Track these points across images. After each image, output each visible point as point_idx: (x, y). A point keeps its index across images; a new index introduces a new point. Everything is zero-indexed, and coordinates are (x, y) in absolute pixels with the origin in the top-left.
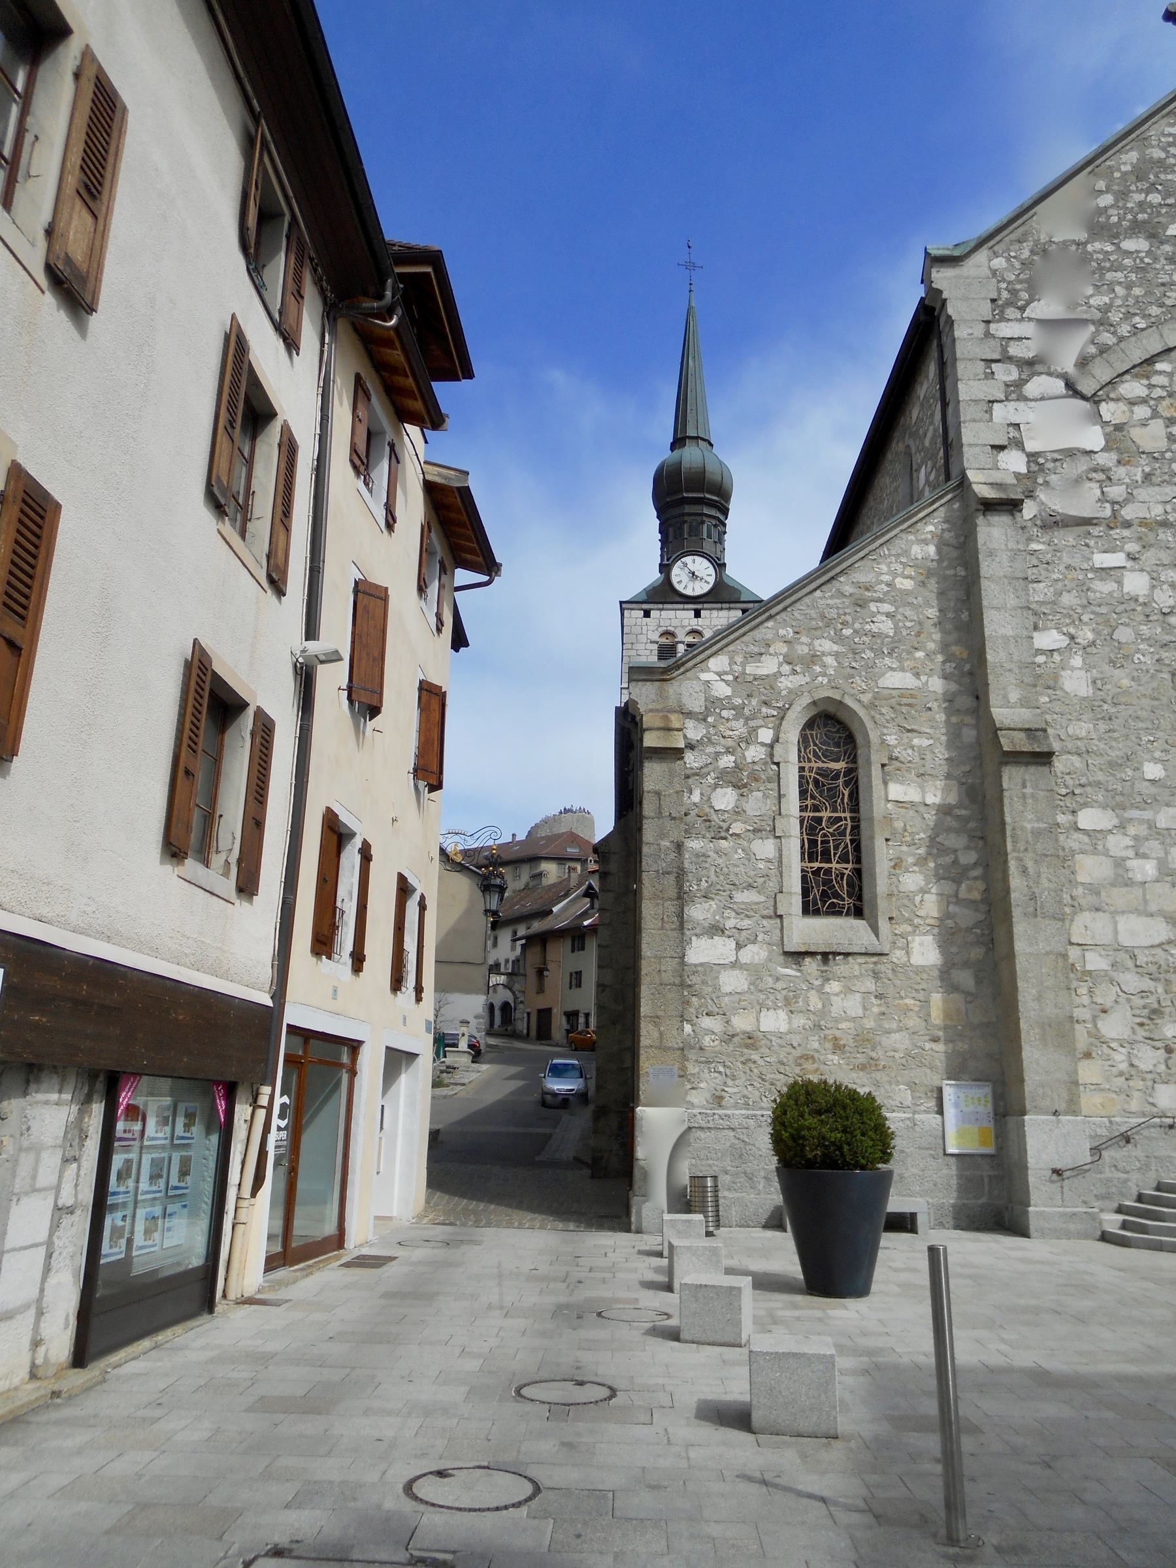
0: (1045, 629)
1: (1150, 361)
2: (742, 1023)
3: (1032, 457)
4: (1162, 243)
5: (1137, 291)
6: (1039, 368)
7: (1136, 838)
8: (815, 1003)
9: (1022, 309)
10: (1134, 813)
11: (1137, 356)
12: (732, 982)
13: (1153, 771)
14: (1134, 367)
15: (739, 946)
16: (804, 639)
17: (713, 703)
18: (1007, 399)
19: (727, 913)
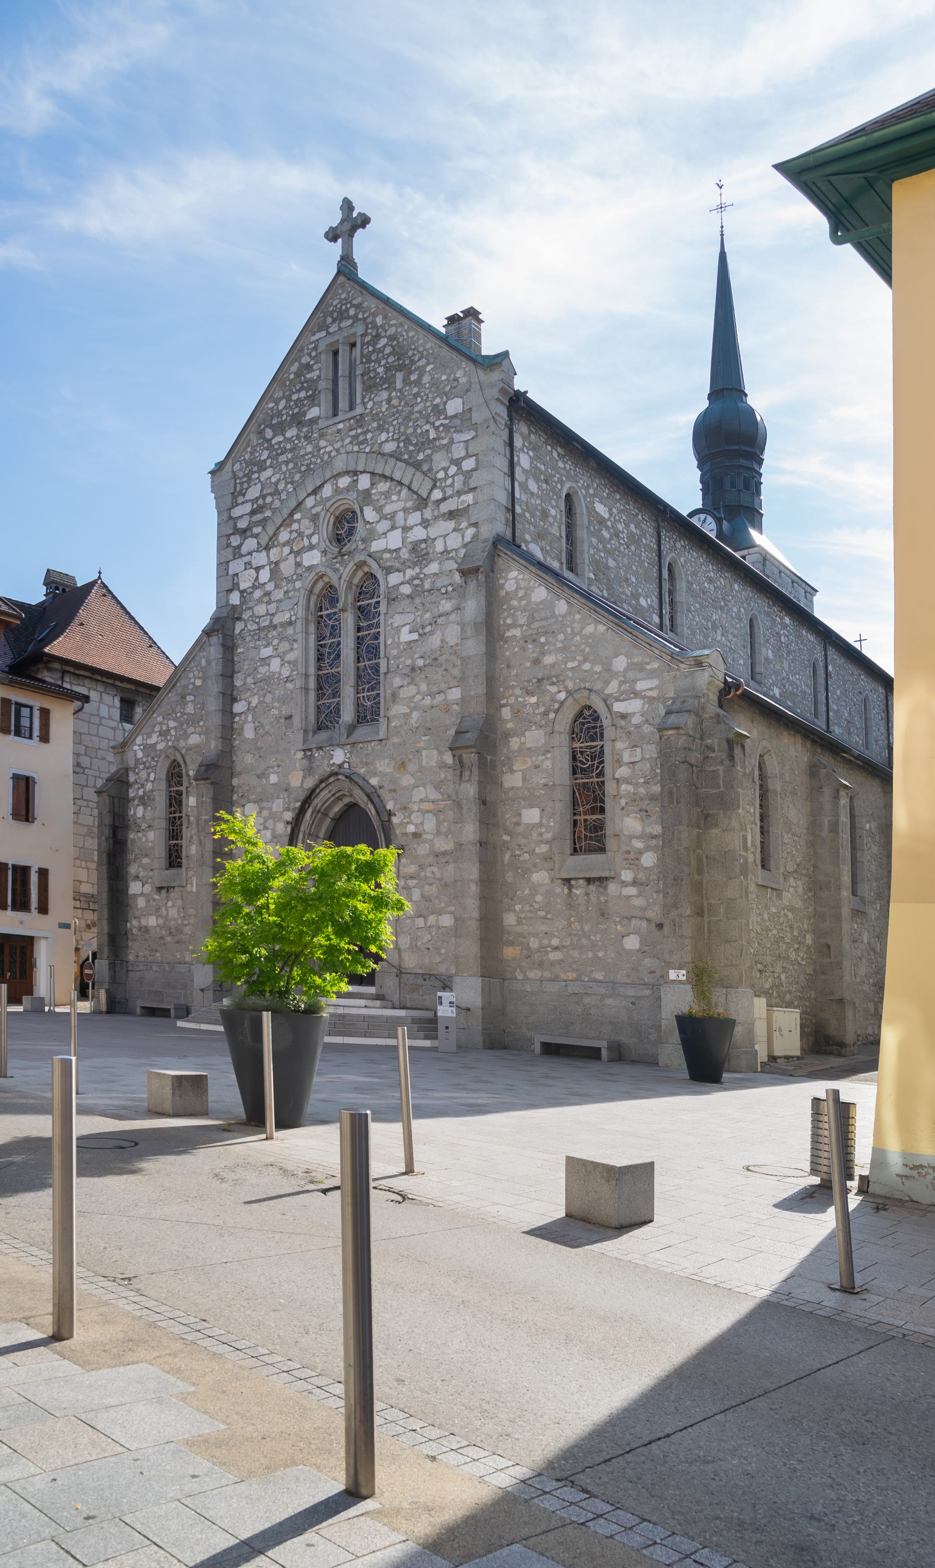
0: (241, 700)
1: (291, 514)
2: (144, 922)
3: (242, 592)
4: (303, 426)
5: (291, 465)
6: (249, 533)
7: (264, 818)
8: (164, 913)
9: (244, 495)
10: (265, 804)
11: (286, 512)
12: (141, 903)
13: (274, 779)
14: (284, 520)
15: (143, 885)
16: (166, 722)
17: (137, 760)
18: (235, 559)
19: (141, 869)
